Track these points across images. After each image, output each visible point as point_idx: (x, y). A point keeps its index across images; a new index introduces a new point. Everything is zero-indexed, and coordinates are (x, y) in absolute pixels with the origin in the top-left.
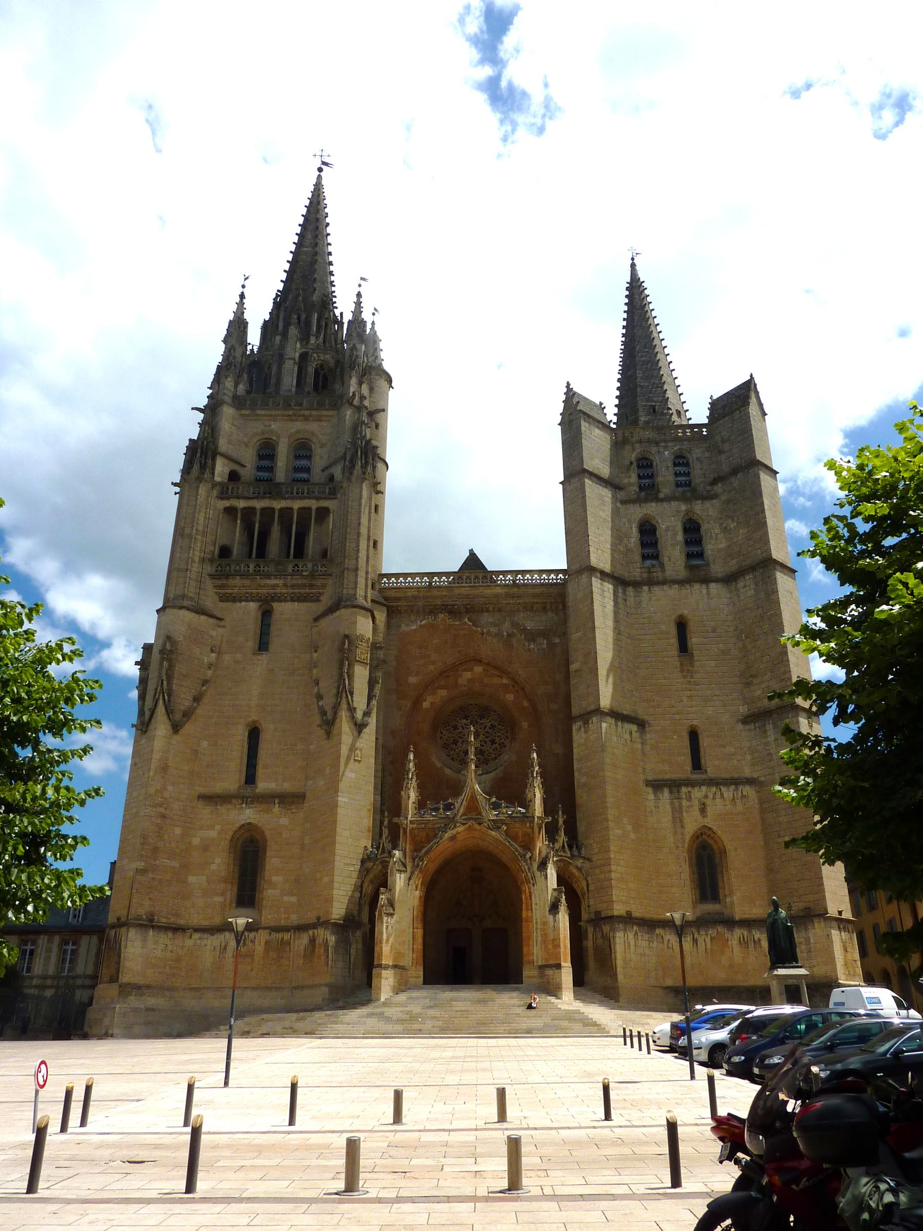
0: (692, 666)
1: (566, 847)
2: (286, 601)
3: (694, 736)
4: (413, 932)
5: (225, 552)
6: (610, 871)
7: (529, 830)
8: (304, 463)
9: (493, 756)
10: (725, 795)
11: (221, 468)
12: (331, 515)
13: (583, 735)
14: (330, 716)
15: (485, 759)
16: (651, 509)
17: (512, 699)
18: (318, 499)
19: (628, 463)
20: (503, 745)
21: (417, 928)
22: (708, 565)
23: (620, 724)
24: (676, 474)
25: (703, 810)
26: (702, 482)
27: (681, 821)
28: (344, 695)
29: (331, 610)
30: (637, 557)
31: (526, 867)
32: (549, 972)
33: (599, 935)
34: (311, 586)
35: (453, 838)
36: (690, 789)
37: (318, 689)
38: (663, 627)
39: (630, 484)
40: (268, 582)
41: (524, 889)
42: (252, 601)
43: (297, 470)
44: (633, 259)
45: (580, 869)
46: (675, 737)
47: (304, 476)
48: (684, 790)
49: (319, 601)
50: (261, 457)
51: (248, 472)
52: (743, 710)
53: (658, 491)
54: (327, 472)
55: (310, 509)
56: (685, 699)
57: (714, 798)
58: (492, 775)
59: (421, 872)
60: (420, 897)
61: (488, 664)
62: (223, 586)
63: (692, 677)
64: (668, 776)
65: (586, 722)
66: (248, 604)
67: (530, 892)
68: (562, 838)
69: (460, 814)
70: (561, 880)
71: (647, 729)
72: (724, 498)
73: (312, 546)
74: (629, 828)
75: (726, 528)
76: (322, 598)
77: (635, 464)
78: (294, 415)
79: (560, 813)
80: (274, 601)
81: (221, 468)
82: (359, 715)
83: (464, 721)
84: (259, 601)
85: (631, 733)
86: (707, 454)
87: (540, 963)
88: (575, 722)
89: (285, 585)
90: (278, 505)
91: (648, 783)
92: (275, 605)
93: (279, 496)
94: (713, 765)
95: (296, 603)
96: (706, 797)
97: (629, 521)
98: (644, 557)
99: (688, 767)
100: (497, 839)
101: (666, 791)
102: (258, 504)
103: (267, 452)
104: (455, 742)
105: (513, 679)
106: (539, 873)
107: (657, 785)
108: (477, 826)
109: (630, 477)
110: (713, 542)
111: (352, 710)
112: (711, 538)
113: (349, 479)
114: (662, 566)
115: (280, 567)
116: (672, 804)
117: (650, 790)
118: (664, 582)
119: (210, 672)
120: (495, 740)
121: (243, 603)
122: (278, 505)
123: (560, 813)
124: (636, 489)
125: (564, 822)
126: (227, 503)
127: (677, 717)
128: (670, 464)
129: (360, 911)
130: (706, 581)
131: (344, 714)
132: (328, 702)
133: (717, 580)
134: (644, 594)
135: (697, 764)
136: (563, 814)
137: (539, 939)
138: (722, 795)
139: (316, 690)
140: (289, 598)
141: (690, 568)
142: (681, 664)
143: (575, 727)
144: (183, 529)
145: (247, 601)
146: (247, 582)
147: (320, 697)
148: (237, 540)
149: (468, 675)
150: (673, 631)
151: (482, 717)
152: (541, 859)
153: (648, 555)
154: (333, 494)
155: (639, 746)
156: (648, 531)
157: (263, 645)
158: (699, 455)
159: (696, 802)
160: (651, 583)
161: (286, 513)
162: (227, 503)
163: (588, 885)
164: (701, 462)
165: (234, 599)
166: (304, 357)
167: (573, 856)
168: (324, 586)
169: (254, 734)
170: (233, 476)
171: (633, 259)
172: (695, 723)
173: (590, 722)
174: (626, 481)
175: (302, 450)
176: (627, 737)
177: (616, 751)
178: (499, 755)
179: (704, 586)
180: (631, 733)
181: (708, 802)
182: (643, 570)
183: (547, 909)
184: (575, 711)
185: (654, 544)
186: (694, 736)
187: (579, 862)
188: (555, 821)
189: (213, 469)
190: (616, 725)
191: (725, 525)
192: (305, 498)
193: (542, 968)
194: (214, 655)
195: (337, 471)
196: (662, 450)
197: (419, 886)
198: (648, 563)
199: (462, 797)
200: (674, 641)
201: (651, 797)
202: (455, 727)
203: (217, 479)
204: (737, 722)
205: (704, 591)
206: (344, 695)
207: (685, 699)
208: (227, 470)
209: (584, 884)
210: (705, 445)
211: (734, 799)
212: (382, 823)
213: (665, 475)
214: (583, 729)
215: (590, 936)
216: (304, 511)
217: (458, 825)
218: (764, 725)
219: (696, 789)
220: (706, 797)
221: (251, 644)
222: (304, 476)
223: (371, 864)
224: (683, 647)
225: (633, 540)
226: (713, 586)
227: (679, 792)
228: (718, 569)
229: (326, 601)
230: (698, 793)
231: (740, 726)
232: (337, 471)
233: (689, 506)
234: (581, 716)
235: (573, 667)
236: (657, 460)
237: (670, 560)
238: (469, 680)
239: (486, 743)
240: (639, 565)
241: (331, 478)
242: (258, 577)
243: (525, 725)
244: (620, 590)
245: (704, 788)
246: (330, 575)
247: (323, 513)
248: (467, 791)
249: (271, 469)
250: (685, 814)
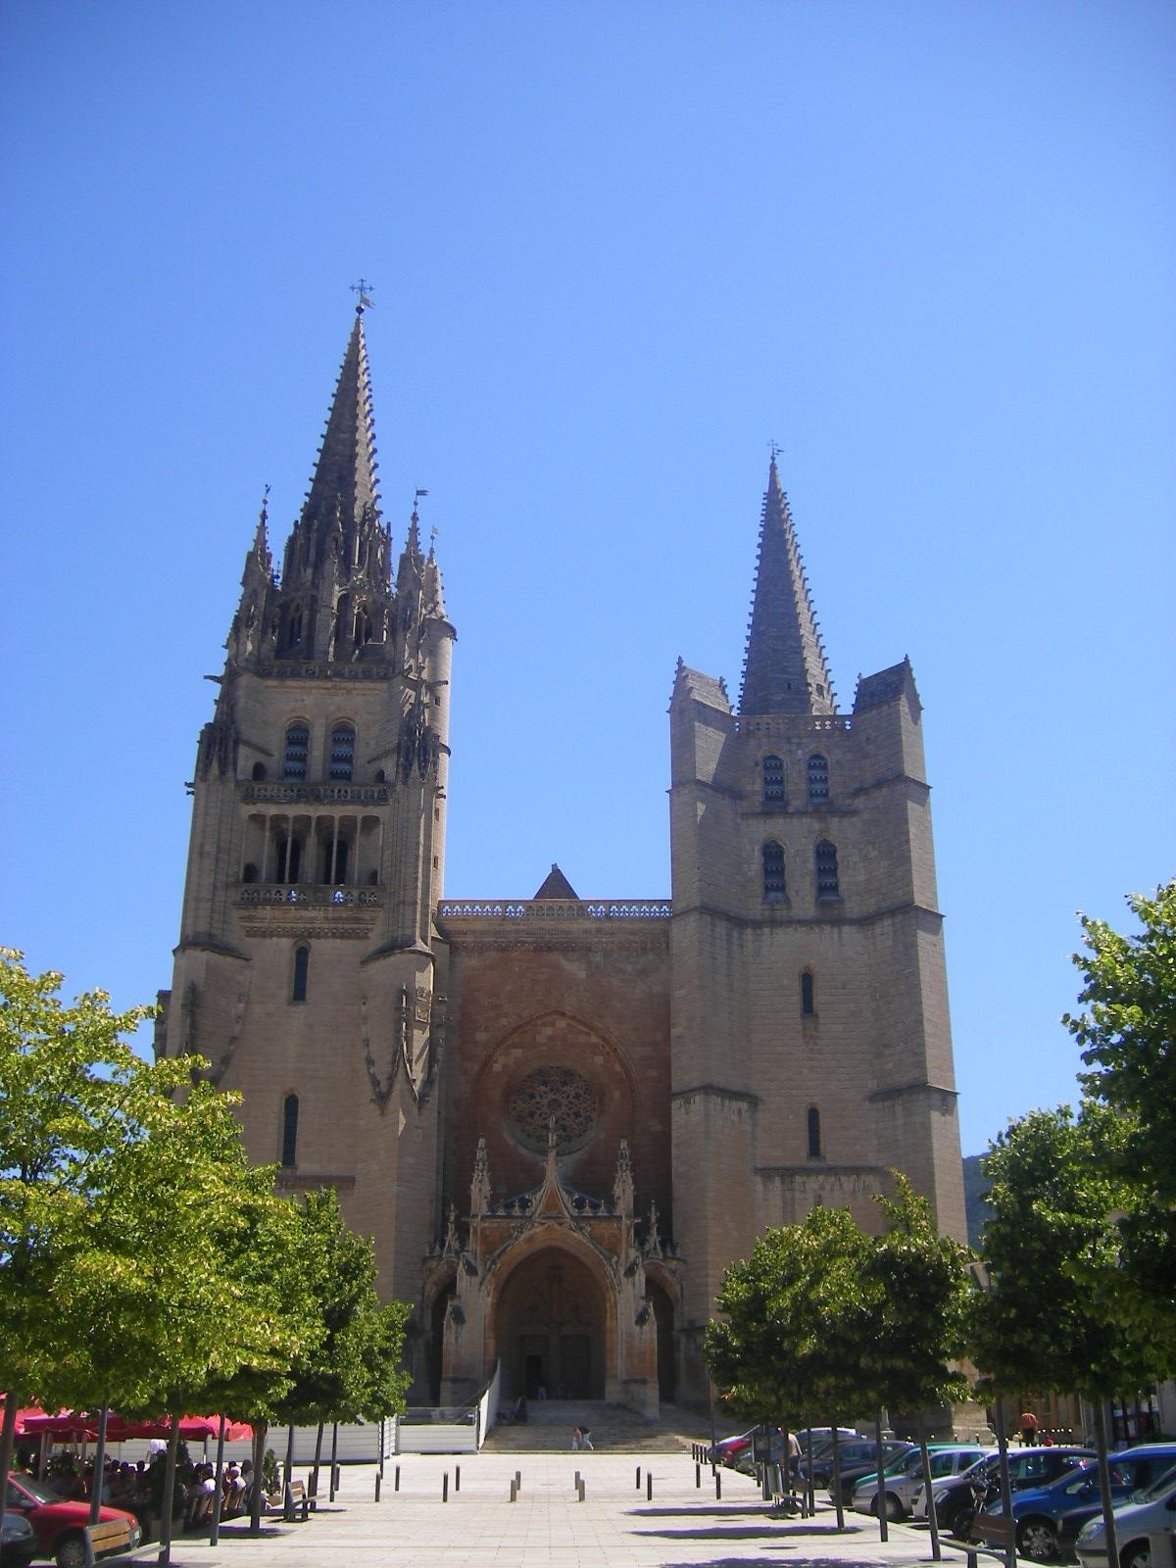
1: (659, 1248)
2: (326, 937)
3: (813, 1115)
4: (485, 1343)
5: (251, 873)
6: (707, 1276)
7: (616, 1232)
8: (344, 750)
9: (577, 1132)
10: (845, 1186)
11: (246, 759)
12: (381, 826)
13: (684, 1116)
14: (384, 1087)
15: (567, 1136)
16: (775, 827)
17: (602, 1062)
18: (365, 804)
20: (589, 1119)
21: (490, 1338)
22: (841, 901)
23: (727, 1102)
24: (811, 781)
28: (401, 1064)
29: (385, 952)
30: (758, 889)
31: (612, 1273)
32: (634, 1387)
33: (692, 1346)
34: (358, 920)
35: (530, 1240)
36: (805, 1178)
37: (369, 1052)
40: (304, 913)
41: (608, 1296)
42: (284, 936)
43: (336, 759)
44: (773, 459)
45: (674, 1272)
46: (791, 1117)
47: (345, 767)
48: (798, 1179)
49: (368, 938)
50: (291, 742)
51: (275, 763)
52: (872, 1085)
53: (788, 804)
54: (375, 766)
55: (354, 819)
56: (805, 1071)
57: (832, 1190)
58: (576, 1156)
59: (494, 1275)
60: (493, 1304)
61: (573, 1018)
62: (251, 918)
63: (815, 1044)
64: (780, 1164)
65: (688, 1102)
66: (280, 940)
67: (615, 1301)
68: (654, 1238)
69: (538, 1212)
70: (649, 1281)
71: (760, 1107)
72: (866, 816)
73: (357, 865)
76: (370, 935)
77: (761, 765)
78: (334, 687)
79: (653, 1209)
80: (311, 938)
81: (246, 759)
83: (542, 1088)
84: (293, 938)
85: (740, 1112)
86: (849, 756)
87: (624, 1378)
88: (675, 1100)
89: (327, 918)
90: (315, 811)
91: (757, 1171)
92: (313, 942)
93: (317, 798)
94: (832, 1149)
95: (338, 940)
96: (822, 1188)
98: (768, 889)
99: (804, 1151)
100: (580, 1241)
101: (777, 1181)
102: (293, 811)
103: (298, 736)
104: (532, 1115)
105: (603, 1038)
106: (626, 1279)
107: (767, 1173)
108: (558, 1227)
113: (405, 782)
114: (787, 901)
117: (758, 1179)
118: (790, 922)
119: (238, 1028)
120: (579, 1112)
121: (274, 939)
122: (315, 811)
123: (653, 1209)
124: (760, 798)
125: (658, 1220)
126: (252, 809)
128: (803, 767)
130: (837, 922)
131: (399, 1086)
132: (382, 1070)
133: (851, 922)
135: (815, 1150)
136: (656, 1211)
137: (624, 1352)
138: (841, 1185)
139: (365, 1053)
140: (330, 934)
141: (821, 904)
142: (804, 1029)
143: (675, 1105)
144: (202, 846)
145: (279, 936)
146: (278, 913)
147: (370, 1062)
148: (263, 852)
149: (549, 1031)
150: (797, 987)
151: (564, 1083)
152: (628, 1265)
153: (772, 885)
154: (382, 799)
155: (748, 1128)
156: (773, 855)
157: (299, 994)
159: (810, 1195)
160: (774, 923)
161: (324, 823)
162: (252, 809)
163: (682, 1290)
165: (265, 934)
166: (345, 601)
167: (665, 1258)
168: (373, 920)
169: (291, 1104)
170: (259, 772)
171: (773, 459)
172: (815, 1100)
173: (692, 1101)
175: (343, 733)
176: (735, 1118)
178: (585, 1131)
179: (836, 930)
180: (740, 1112)
181: (825, 1194)
183: (634, 1319)
184: (675, 1087)
185: (780, 872)
186: (813, 1115)
187: (673, 1264)
188: (647, 1220)
189: (235, 764)
190: (723, 1105)
191: (864, 852)
192: (352, 803)
193: (627, 1383)
194: (242, 1005)
195: (389, 767)
196: (794, 747)
197: (492, 1292)
199: (541, 1193)
200: (797, 999)
201: (760, 1187)
202: (532, 1096)
203: (241, 777)
205: (836, 936)
206: (401, 1064)
207: (805, 1071)
208: (251, 765)
209: (678, 1289)
211: (854, 1191)
212: (445, 1219)
213: (796, 783)
214: (683, 1109)
215: (682, 1347)
216: (348, 823)
217: (536, 1225)
219: (813, 1178)
220: (822, 1188)
221: (285, 992)
222: (345, 767)
223: (435, 1263)
224: (808, 1007)
225: (754, 867)
226: (846, 929)
227: (792, 1182)
228: (853, 908)
229: (375, 941)
230: (813, 1183)
231: (867, 1105)
232: (389, 767)
233: (824, 825)
234: (681, 1093)
235: (675, 1032)
236: (786, 760)
237: (797, 895)
238: (551, 1038)
239: (568, 1115)
240: (760, 900)
241: (380, 776)
242: (293, 908)
243: (617, 1095)
244: (735, 934)
245: (821, 1178)
246: (381, 906)
247: (371, 823)
248: (546, 1185)
249: (302, 759)
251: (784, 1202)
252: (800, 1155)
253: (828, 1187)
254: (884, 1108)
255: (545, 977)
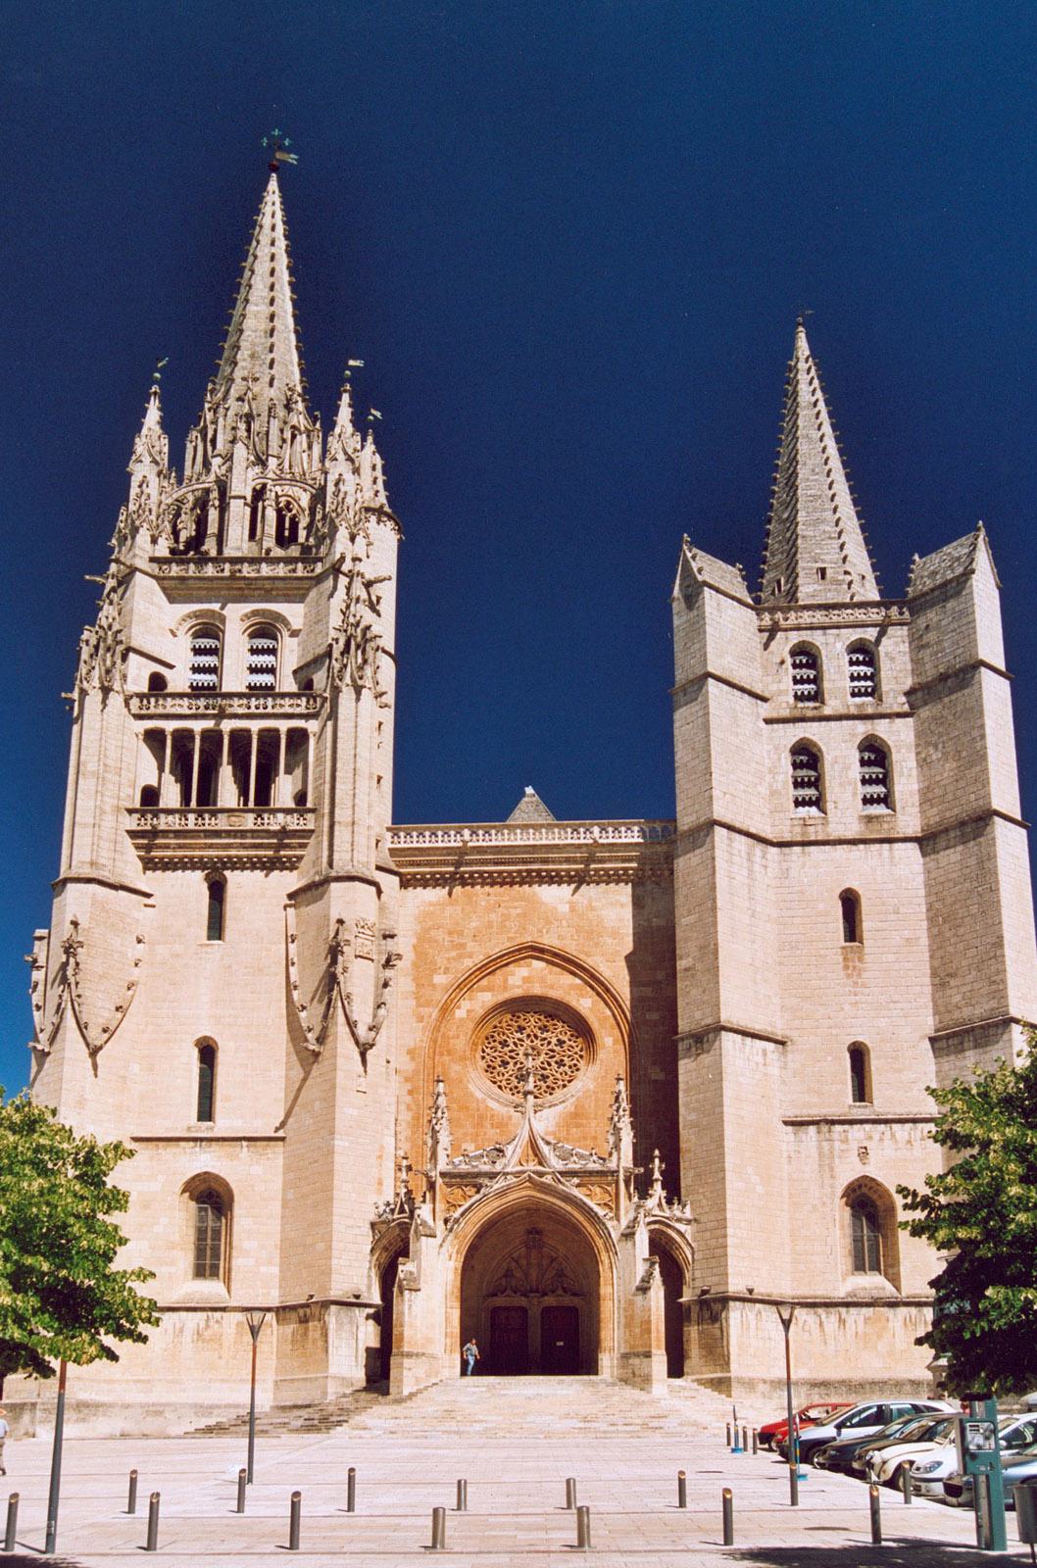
0: (861, 960)
19: (779, 661)
25: (864, 1153)
26: (892, 690)
27: (832, 1169)
38: (821, 906)
39: (780, 693)
46: (829, 1058)
56: (847, 1007)
57: (881, 1140)
63: (859, 975)
74: (755, 1179)
75: (925, 760)
82: (362, 1031)
97: (776, 748)
109: (780, 682)
110: (904, 780)
111: (351, 1025)
112: (902, 774)
115: (233, 819)
116: (820, 1148)
127: (834, 1032)
129: (369, 1287)
134: (794, 858)
138: (893, 1135)
158: (890, 649)
159: (854, 1146)
161: (240, 738)
164: (892, 659)
174: (774, 687)
177: (741, 1079)
182: (796, 822)
198: (803, 811)
204: (922, 1038)
207: (847, 1007)
210: (899, 633)
218: (962, 1043)
224: (852, 931)
225: (780, 778)
233: (870, 727)
250: (837, 1160)
251: (821, 1155)
252: (842, 1100)
253: (876, 1137)
254: (948, 1047)
255: (519, 911)
